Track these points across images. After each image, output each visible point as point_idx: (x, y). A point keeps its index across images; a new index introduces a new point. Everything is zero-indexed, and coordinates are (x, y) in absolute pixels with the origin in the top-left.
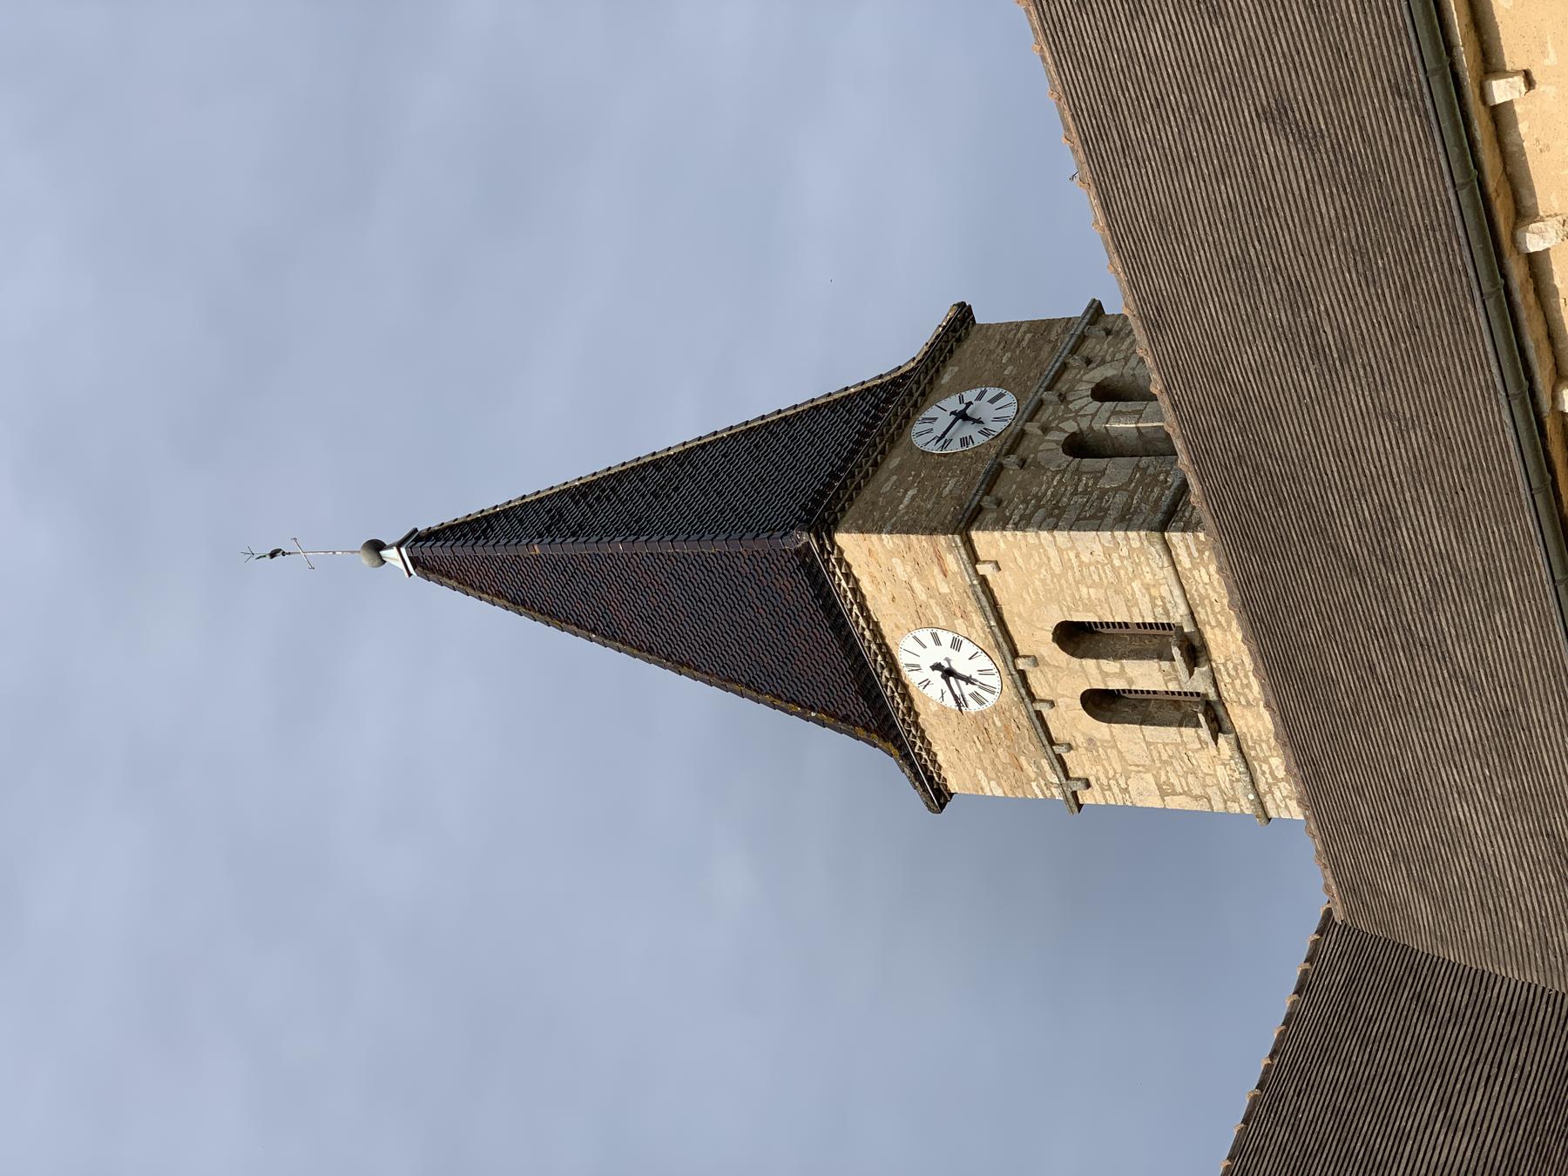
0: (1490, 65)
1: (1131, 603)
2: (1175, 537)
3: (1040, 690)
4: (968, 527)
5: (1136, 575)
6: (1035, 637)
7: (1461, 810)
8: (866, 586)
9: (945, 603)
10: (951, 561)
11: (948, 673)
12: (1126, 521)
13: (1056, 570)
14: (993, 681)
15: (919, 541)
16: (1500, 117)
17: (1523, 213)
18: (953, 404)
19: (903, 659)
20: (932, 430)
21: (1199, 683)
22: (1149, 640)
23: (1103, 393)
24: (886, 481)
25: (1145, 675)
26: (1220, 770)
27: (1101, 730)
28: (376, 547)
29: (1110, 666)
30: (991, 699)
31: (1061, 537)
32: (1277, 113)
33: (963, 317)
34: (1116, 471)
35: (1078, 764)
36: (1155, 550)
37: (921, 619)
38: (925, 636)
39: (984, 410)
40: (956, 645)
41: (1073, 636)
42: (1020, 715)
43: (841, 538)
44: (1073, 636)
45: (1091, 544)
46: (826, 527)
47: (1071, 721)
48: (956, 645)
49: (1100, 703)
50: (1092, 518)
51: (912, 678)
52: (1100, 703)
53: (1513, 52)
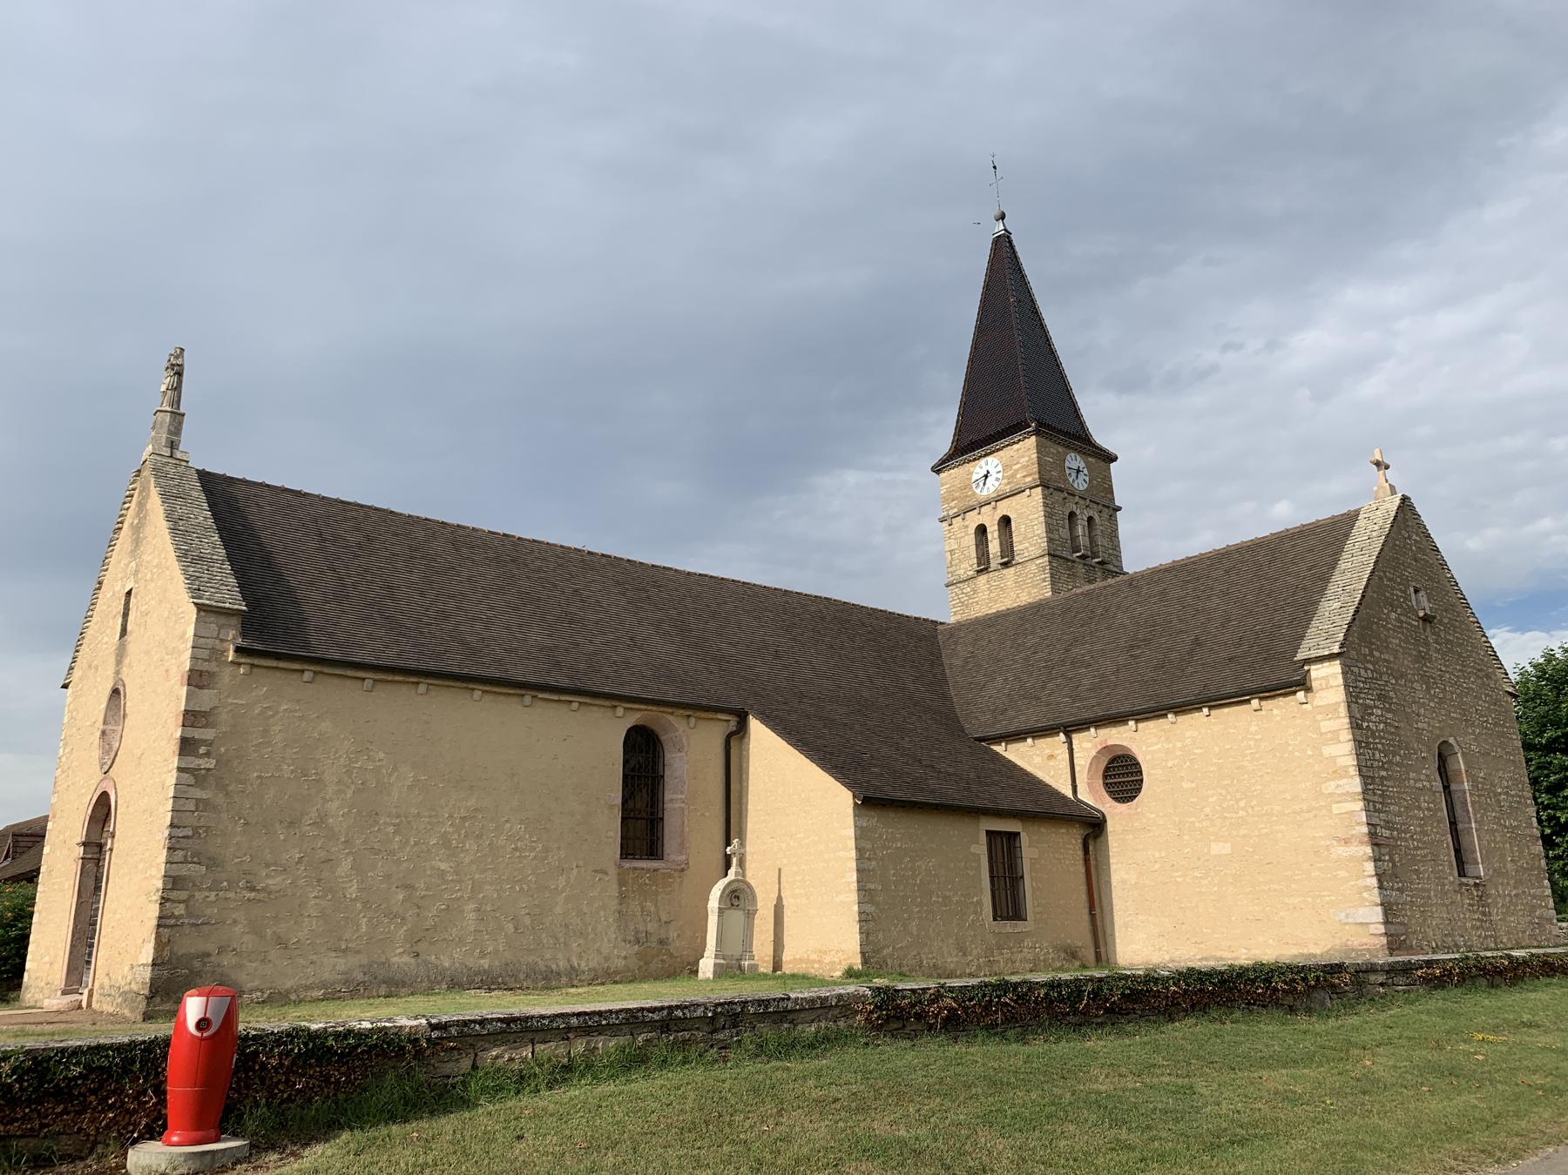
0: (1211, 708)
4: (1044, 484)
6: (1004, 508)
7: (1000, 679)
9: (1013, 476)
10: (1029, 479)
12: (1050, 540)
13: (1029, 514)
14: (985, 493)
15: (1035, 468)
16: (1200, 709)
17: (1176, 714)
18: (1082, 465)
19: (989, 459)
20: (1074, 461)
21: (994, 564)
23: (1090, 519)
24: (1055, 449)
25: (994, 547)
27: (972, 530)
28: (1002, 217)
29: (996, 534)
32: (1197, 642)
34: (1065, 533)
35: (957, 522)
36: (1039, 552)
37: (1006, 467)
38: (1000, 468)
39: (1081, 476)
41: (1006, 521)
42: (973, 503)
43: (1033, 438)
44: (1006, 521)
45: (1041, 529)
46: (1037, 433)
47: (974, 520)
49: (982, 530)
50: (1050, 529)
51: (982, 461)
52: (982, 530)
53: (1213, 712)
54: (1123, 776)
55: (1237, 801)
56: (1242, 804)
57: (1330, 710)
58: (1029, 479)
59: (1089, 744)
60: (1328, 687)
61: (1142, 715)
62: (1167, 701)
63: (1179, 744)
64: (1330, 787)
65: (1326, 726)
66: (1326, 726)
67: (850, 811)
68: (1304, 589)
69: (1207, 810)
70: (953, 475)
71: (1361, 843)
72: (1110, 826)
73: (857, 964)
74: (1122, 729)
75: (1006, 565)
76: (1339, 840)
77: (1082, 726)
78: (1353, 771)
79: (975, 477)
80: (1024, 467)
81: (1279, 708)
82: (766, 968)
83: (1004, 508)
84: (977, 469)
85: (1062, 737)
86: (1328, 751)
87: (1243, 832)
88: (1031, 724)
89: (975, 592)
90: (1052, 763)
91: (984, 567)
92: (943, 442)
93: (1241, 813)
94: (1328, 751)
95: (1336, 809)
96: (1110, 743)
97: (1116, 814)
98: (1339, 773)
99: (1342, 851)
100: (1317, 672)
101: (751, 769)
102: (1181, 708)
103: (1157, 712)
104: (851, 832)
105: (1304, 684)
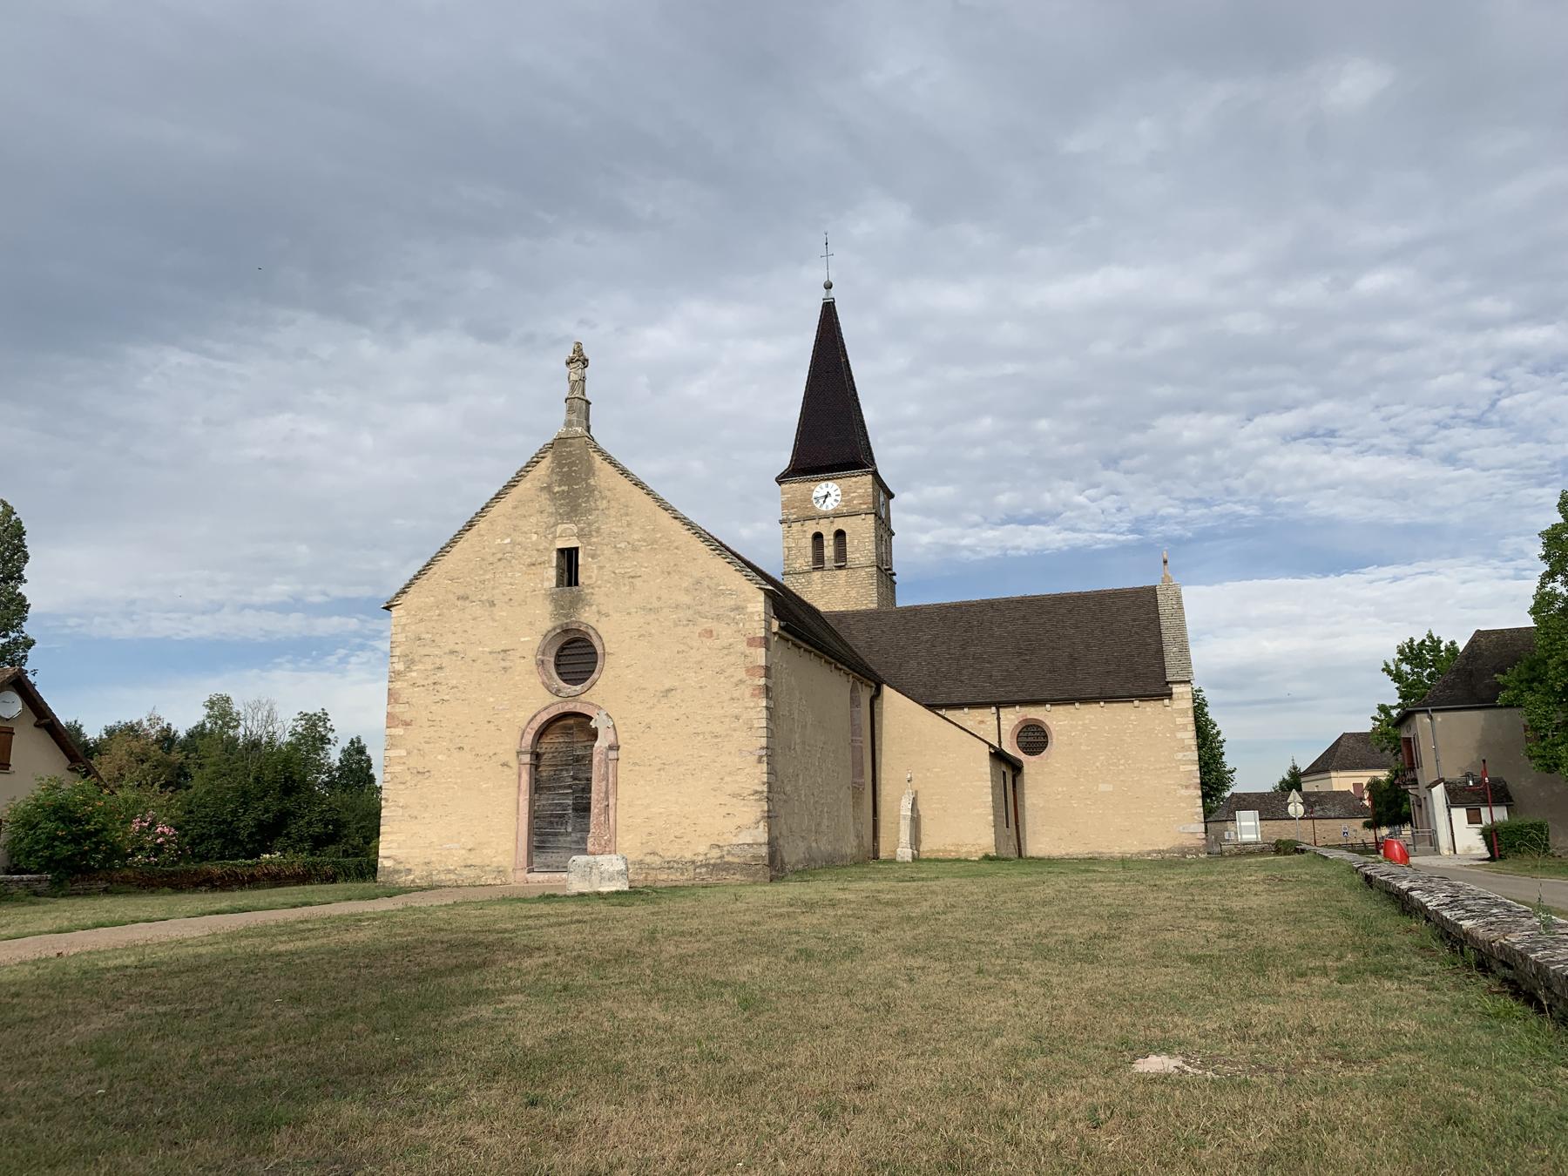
13: (861, 533)
21: (827, 565)
22: (841, 554)
25: (829, 551)
27: (810, 536)
28: (828, 286)
33: (891, 496)
35: (796, 526)
37: (844, 493)
41: (840, 534)
44: (840, 534)
45: (872, 547)
47: (812, 527)
49: (818, 537)
51: (823, 484)
52: (818, 537)
57: (1183, 712)
59: (1012, 718)
61: (1055, 702)
64: (1180, 756)
65: (1179, 721)
67: (987, 756)
70: (796, 488)
72: (1026, 769)
73: (993, 853)
75: (840, 568)
77: (1012, 704)
78: (1194, 748)
81: (1150, 708)
82: (905, 853)
83: (840, 524)
86: (1179, 735)
88: (969, 699)
91: (819, 560)
92: (784, 460)
94: (1179, 735)
95: (1182, 768)
97: (1029, 763)
98: (1184, 748)
99: (1184, 792)
100: (1176, 689)
101: (885, 722)
102: (1084, 701)
103: (1069, 701)
105: (1170, 696)
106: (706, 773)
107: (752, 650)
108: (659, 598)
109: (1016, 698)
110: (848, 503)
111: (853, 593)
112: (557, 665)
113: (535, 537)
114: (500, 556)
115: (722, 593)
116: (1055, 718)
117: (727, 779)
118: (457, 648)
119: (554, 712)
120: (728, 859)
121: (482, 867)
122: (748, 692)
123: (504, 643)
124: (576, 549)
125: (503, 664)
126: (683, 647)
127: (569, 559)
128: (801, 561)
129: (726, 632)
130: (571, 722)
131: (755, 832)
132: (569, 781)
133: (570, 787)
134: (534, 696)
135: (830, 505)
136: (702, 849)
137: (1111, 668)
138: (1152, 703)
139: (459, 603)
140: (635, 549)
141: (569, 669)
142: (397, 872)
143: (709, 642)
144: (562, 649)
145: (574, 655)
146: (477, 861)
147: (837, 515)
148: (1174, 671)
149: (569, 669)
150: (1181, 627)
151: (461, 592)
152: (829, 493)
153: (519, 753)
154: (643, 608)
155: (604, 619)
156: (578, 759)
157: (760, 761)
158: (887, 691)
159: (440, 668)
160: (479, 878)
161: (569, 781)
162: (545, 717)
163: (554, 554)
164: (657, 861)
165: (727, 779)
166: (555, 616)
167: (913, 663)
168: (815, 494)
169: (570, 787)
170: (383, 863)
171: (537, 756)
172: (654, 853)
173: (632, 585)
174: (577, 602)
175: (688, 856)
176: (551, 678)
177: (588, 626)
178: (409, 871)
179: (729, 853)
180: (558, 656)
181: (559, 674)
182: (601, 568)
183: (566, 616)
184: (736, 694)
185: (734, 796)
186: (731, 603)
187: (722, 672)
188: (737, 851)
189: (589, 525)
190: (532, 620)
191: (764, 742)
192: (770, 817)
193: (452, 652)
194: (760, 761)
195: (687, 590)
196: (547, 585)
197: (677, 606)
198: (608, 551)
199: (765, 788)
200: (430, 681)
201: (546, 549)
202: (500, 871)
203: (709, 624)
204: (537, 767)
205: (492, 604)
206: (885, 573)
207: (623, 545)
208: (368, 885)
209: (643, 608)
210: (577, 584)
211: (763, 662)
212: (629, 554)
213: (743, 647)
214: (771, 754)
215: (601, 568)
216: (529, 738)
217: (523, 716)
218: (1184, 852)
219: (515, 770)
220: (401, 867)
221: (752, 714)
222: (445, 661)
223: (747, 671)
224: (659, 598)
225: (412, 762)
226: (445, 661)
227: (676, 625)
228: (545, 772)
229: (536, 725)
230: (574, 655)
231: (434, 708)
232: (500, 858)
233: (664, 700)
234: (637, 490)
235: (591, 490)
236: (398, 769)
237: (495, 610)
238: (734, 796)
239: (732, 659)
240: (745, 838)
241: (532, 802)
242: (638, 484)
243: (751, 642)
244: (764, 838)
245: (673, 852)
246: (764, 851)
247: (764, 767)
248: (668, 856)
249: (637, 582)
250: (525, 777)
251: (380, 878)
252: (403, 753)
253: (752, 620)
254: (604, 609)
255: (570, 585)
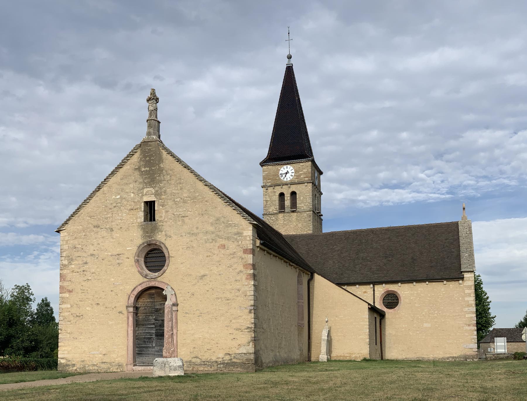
1: (300, 204)
2: (312, 212)
3: (284, 186)
4: (313, 184)
5: (305, 206)
6: (293, 188)
8: (301, 164)
10: (307, 179)
11: (286, 173)
13: (305, 193)
14: (285, 180)
15: (310, 175)
19: (289, 166)
21: (287, 210)
26: (271, 210)
27: (277, 194)
29: (289, 198)
30: (282, 178)
31: (311, 196)
33: (321, 173)
35: (270, 189)
37: (296, 171)
38: (293, 171)
40: (292, 176)
41: (293, 194)
44: (293, 194)
48: (292, 176)
49: (282, 195)
51: (285, 167)
52: (282, 195)
54: (392, 301)
55: (434, 311)
56: (436, 312)
57: (469, 287)
58: (307, 179)
60: (469, 280)
61: (403, 282)
62: (415, 278)
63: (416, 292)
65: (467, 291)
66: (467, 291)
67: (367, 310)
68: (447, 246)
69: (424, 313)
70: (271, 168)
71: (474, 326)
74: (396, 285)
75: (293, 212)
76: (466, 324)
77: (381, 283)
78: (474, 305)
79: (281, 172)
80: (304, 173)
81: (452, 285)
83: (293, 188)
84: (282, 169)
85: (372, 286)
86: (466, 299)
87: (435, 320)
89: (277, 220)
90: (365, 294)
93: (435, 315)
94: (466, 299)
95: (467, 316)
96: (390, 289)
98: (469, 306)
99: (468, 328)
100: (466, 275)
103: (410, 281)
104: (367, 316)
105: (462, 278)
106: (223, 318)
107: (246, 256)
108: (197, 228)
109: (383, 280)
110: (298, 177)
111: (300, 225)
112: (146, 262)
113: (132, 195)
114: (115, 205)
115: (230, 225)
116: (403, 291)
117: (233, 321)
118: (94, 253)
119: (144, 286)
120: (234, 360)
121: (110, 363)
122: (244, 277)
123: (118, 250)
124: (154, 202)
125: (118, 261)
126: (209, 254)
127: (150, 206)
128: (273, 208)
129: (232, 246)
130: (153, 291)
131: (248, 348)
132: (153, 321)
133: (154, 324)
134: (133, 278)
135: (289, 178)
136: (221, 355)
137: (433, 264)
138: (453, 283)
139: (95, 229)
140: (185, 202)
141: (152, 264)
142: (67, 365)
143: (223, 251)
144: (148, 254)
145: (154, 257)
146: (108, 360)
147: (292, 183)
148: (465, 266)
149: (152, 264)
150: (471, 243)
151: (95, 223)
152: (288, 171)
153: (127, 307)
154: (189, 233)
155: (168, 239)
156: (157, 310)
157: (250, 312)
158: (317, 277)
159: (86, 263)
160: (109, 368)
161: (153, 321)
162: (140, 289)
163: (143, 204)
164: (198, 361)
165: (233, 321)
166: (144, 237)
167: (331, 262)
168: (281, 172)
169: (154, 324)
170: (61, 361)
171: (136, 308)
172: (196, 357)
173: (183, 221)
174: (155, 230)
175: (214, 359)
176: (142, 269)
177: (160, 242)
178: (74, 365)
179: (234, 357)
180: (146, 258)
181: (147, 267)
182: (167, 212)
183: (149, 237)
184: (238, 278)
185: (237, 329)
186: (235, 230)
187: (231, 266)
188: (238, 356)
189: (161, 188)
190: (131, 239)
191: (252, 302)
192: (255, 340)
193: (92, 255)
194: (250, 312)
195: (212, 224)
196: (139, 220)
197: (207, 232)
198: (170, 203)
199: (253, 326)
200: (82, 269)
201: (138, 201)
202: (120, 365)
203: (223, 242)
204: (137, 314)
205: (112, 230)
206: (317, 214)
207: (178, 200)
208: (53, 372)
209: (189, 233)
210: (154, 220)
211: (251, 261)
212: (182, 204)
213: (240, 254)
214: (256, 309)
215: (167, 212)
216: (132, 299)
217: (129, 288)
218: (466, 358)
219: (126, 315)
220: (69, 363)
221: (247, 288)
222: (89, 260)
223: (244, 266)
224: (197, 228)
225: (73, 311)
226: (89, 260)
227: (206, 242)
228: (141, 317)
229: (136, 293)
230: (154, 257)
231: (84, 283)
232: (119, 359)
233: (201, 281)
234: (185, 170)
235: (161, 170)
236: (66, 314)
237: (113, 233)
238: (237, 329)
239: (235, 260)
240: (243, 350)
241: (135, 332)
242: (186, 167)
243: (245, 251)
244: (252, 350)
245: (206, 356)
246: (252, 357)
247: (252, 315)
248: (204, 359)
249: (186, 219)
250: (131, 319)
251: (59, 368)
252: (69, 306)
253: (246, 240)
254: (169, 233)
255: (151, 220)
